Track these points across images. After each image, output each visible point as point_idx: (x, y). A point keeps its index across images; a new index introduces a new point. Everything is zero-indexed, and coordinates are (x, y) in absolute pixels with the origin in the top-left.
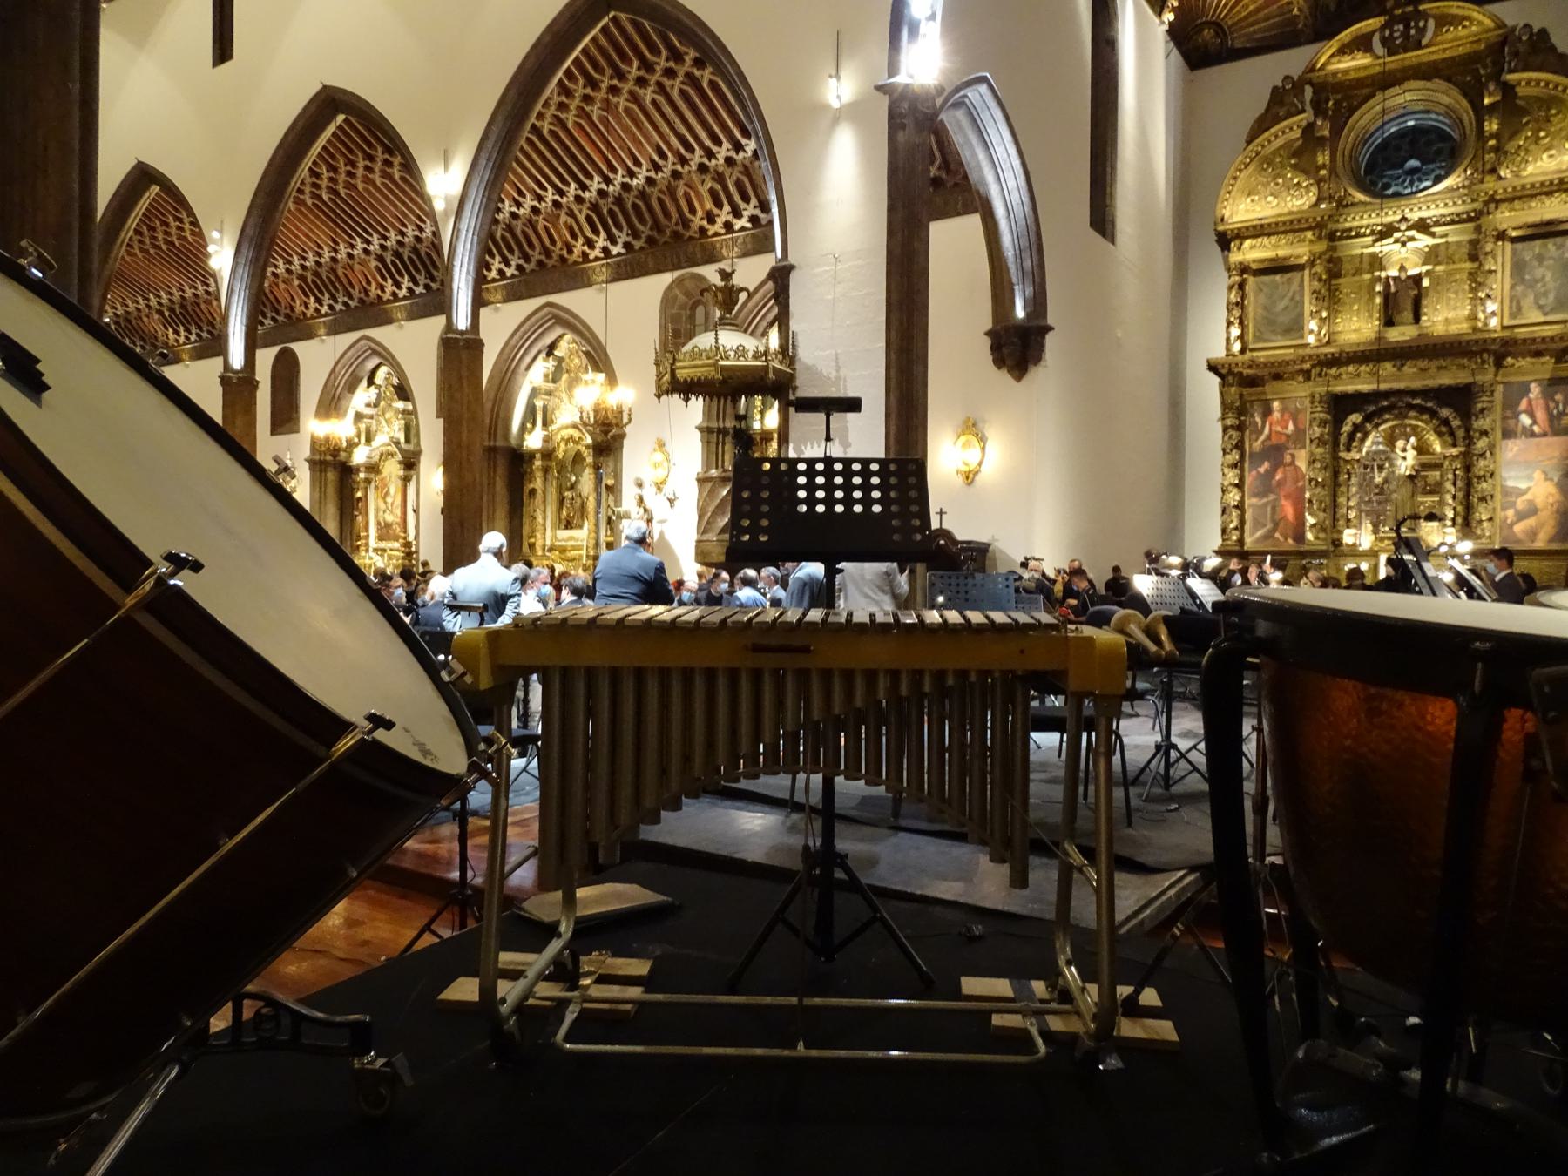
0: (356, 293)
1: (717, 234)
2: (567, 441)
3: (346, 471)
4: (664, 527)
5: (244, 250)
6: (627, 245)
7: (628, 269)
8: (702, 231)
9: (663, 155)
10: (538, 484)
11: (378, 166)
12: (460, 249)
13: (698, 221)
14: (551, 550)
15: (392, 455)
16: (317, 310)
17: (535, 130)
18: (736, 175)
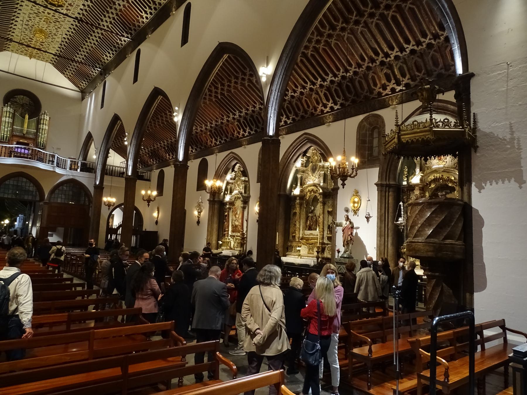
0: (229, 136)
1: (387, 95)
2: (310, 192)
3: (222, 204)
4: (358, 231)
5: (187, 114)
6: (342, 105)
7: (342, 115)
8: (380, 94)
9: (363, 59)
10: (297, 210)
11: (239, 81)
12: (272, 99)
13: (378, 89)
14: (302, 239)
15: (239, 198)
16: (215, 143)
17: (304, 55)
18: (400, 64)
